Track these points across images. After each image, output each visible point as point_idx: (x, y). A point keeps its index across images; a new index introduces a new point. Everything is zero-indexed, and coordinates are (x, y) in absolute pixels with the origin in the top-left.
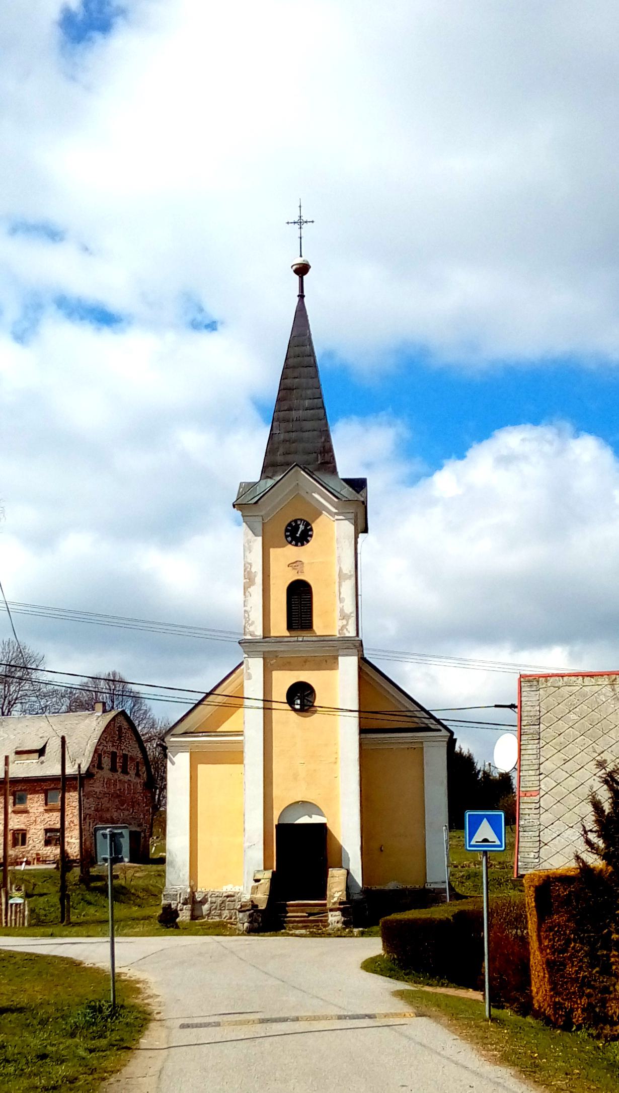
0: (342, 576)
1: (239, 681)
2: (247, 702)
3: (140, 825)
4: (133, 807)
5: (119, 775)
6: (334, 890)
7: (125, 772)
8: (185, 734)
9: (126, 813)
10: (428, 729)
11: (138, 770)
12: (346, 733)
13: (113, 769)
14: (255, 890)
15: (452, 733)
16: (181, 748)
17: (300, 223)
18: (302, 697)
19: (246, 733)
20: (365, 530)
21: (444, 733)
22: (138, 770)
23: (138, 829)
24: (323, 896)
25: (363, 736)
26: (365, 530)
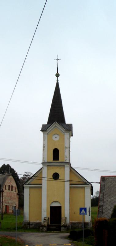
0: (66, 148)
1: (41, 171)
2: (43, 179)
3: (16, 204)
4: (14, 199)
5: (10, 191)
6: (62, 222)
7: (12, 190)
8: (29, 184)
9: (12, 201)
10: (86, 184)
11: (15, 190)
12: (67, 185)
13: (9, 190)
14: (44, 222)
15: (92, 185)
16: (27, 187)
17: (57, 60)
18: (56, 176)
19: (43, 184)
20: (72, 136)
21: (90, 185)
22: (15, 190)
23: (15, 206)
24: (60, 224)
25: (71, 185)
26: (72, 136)
